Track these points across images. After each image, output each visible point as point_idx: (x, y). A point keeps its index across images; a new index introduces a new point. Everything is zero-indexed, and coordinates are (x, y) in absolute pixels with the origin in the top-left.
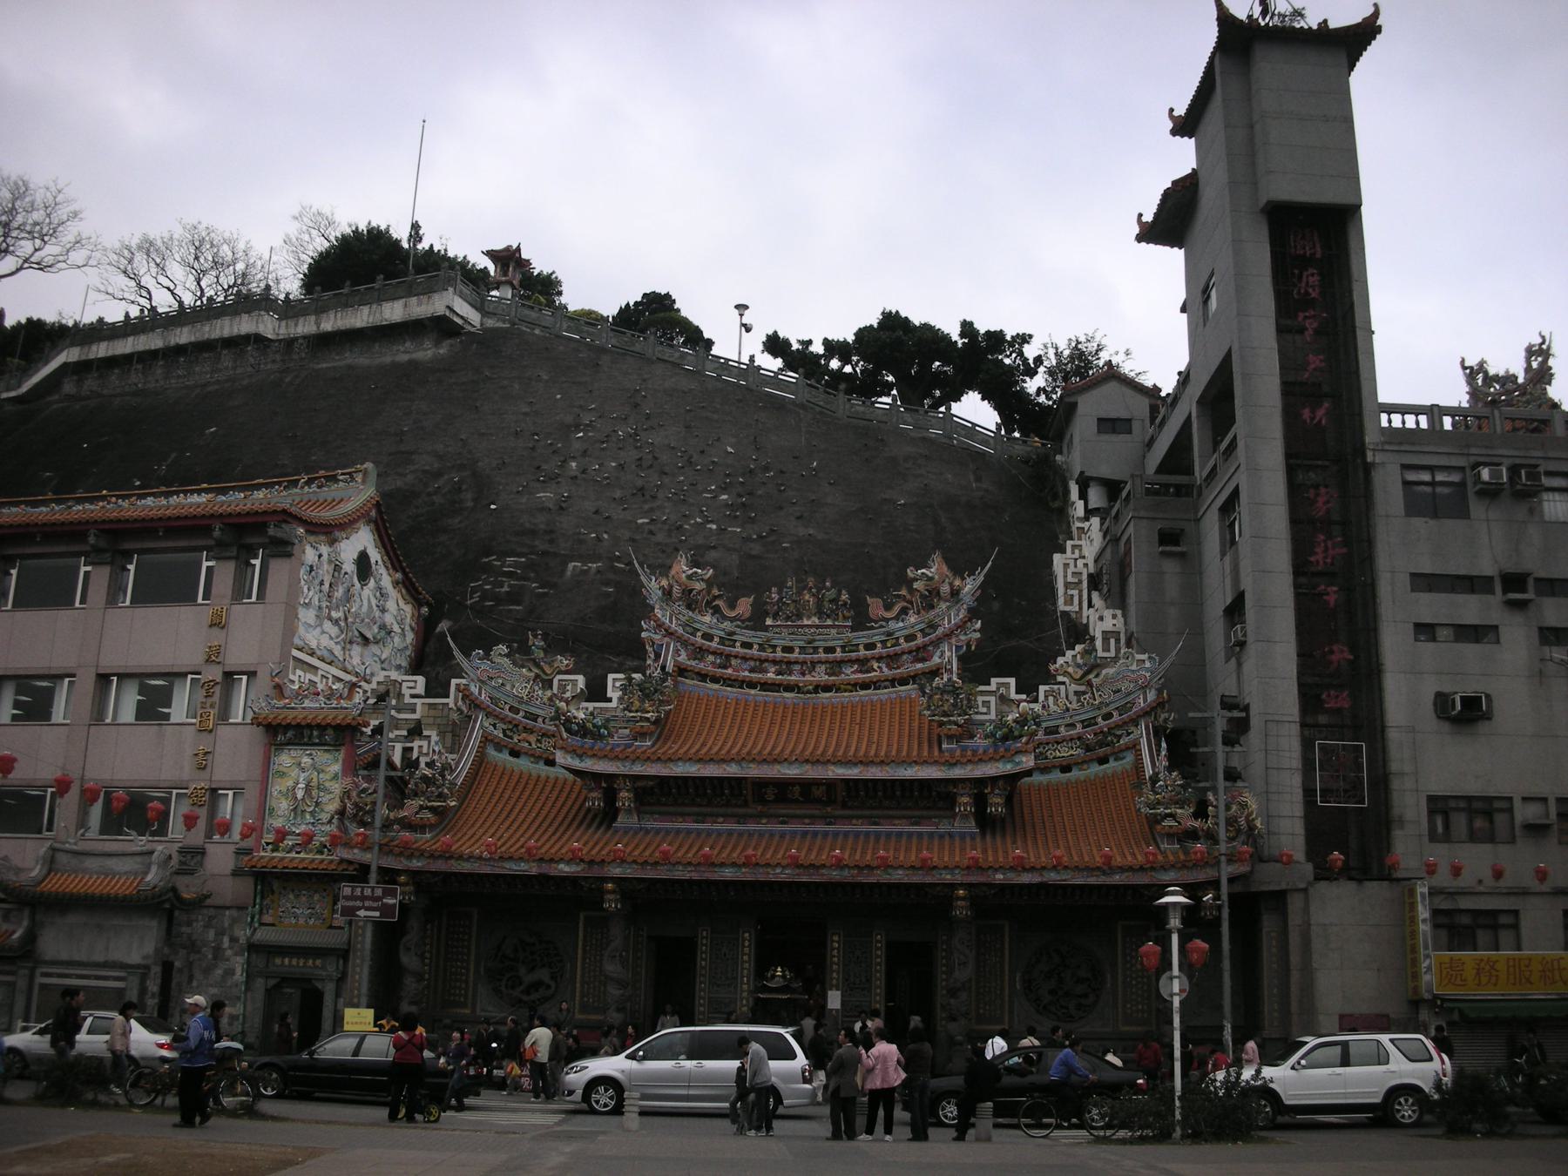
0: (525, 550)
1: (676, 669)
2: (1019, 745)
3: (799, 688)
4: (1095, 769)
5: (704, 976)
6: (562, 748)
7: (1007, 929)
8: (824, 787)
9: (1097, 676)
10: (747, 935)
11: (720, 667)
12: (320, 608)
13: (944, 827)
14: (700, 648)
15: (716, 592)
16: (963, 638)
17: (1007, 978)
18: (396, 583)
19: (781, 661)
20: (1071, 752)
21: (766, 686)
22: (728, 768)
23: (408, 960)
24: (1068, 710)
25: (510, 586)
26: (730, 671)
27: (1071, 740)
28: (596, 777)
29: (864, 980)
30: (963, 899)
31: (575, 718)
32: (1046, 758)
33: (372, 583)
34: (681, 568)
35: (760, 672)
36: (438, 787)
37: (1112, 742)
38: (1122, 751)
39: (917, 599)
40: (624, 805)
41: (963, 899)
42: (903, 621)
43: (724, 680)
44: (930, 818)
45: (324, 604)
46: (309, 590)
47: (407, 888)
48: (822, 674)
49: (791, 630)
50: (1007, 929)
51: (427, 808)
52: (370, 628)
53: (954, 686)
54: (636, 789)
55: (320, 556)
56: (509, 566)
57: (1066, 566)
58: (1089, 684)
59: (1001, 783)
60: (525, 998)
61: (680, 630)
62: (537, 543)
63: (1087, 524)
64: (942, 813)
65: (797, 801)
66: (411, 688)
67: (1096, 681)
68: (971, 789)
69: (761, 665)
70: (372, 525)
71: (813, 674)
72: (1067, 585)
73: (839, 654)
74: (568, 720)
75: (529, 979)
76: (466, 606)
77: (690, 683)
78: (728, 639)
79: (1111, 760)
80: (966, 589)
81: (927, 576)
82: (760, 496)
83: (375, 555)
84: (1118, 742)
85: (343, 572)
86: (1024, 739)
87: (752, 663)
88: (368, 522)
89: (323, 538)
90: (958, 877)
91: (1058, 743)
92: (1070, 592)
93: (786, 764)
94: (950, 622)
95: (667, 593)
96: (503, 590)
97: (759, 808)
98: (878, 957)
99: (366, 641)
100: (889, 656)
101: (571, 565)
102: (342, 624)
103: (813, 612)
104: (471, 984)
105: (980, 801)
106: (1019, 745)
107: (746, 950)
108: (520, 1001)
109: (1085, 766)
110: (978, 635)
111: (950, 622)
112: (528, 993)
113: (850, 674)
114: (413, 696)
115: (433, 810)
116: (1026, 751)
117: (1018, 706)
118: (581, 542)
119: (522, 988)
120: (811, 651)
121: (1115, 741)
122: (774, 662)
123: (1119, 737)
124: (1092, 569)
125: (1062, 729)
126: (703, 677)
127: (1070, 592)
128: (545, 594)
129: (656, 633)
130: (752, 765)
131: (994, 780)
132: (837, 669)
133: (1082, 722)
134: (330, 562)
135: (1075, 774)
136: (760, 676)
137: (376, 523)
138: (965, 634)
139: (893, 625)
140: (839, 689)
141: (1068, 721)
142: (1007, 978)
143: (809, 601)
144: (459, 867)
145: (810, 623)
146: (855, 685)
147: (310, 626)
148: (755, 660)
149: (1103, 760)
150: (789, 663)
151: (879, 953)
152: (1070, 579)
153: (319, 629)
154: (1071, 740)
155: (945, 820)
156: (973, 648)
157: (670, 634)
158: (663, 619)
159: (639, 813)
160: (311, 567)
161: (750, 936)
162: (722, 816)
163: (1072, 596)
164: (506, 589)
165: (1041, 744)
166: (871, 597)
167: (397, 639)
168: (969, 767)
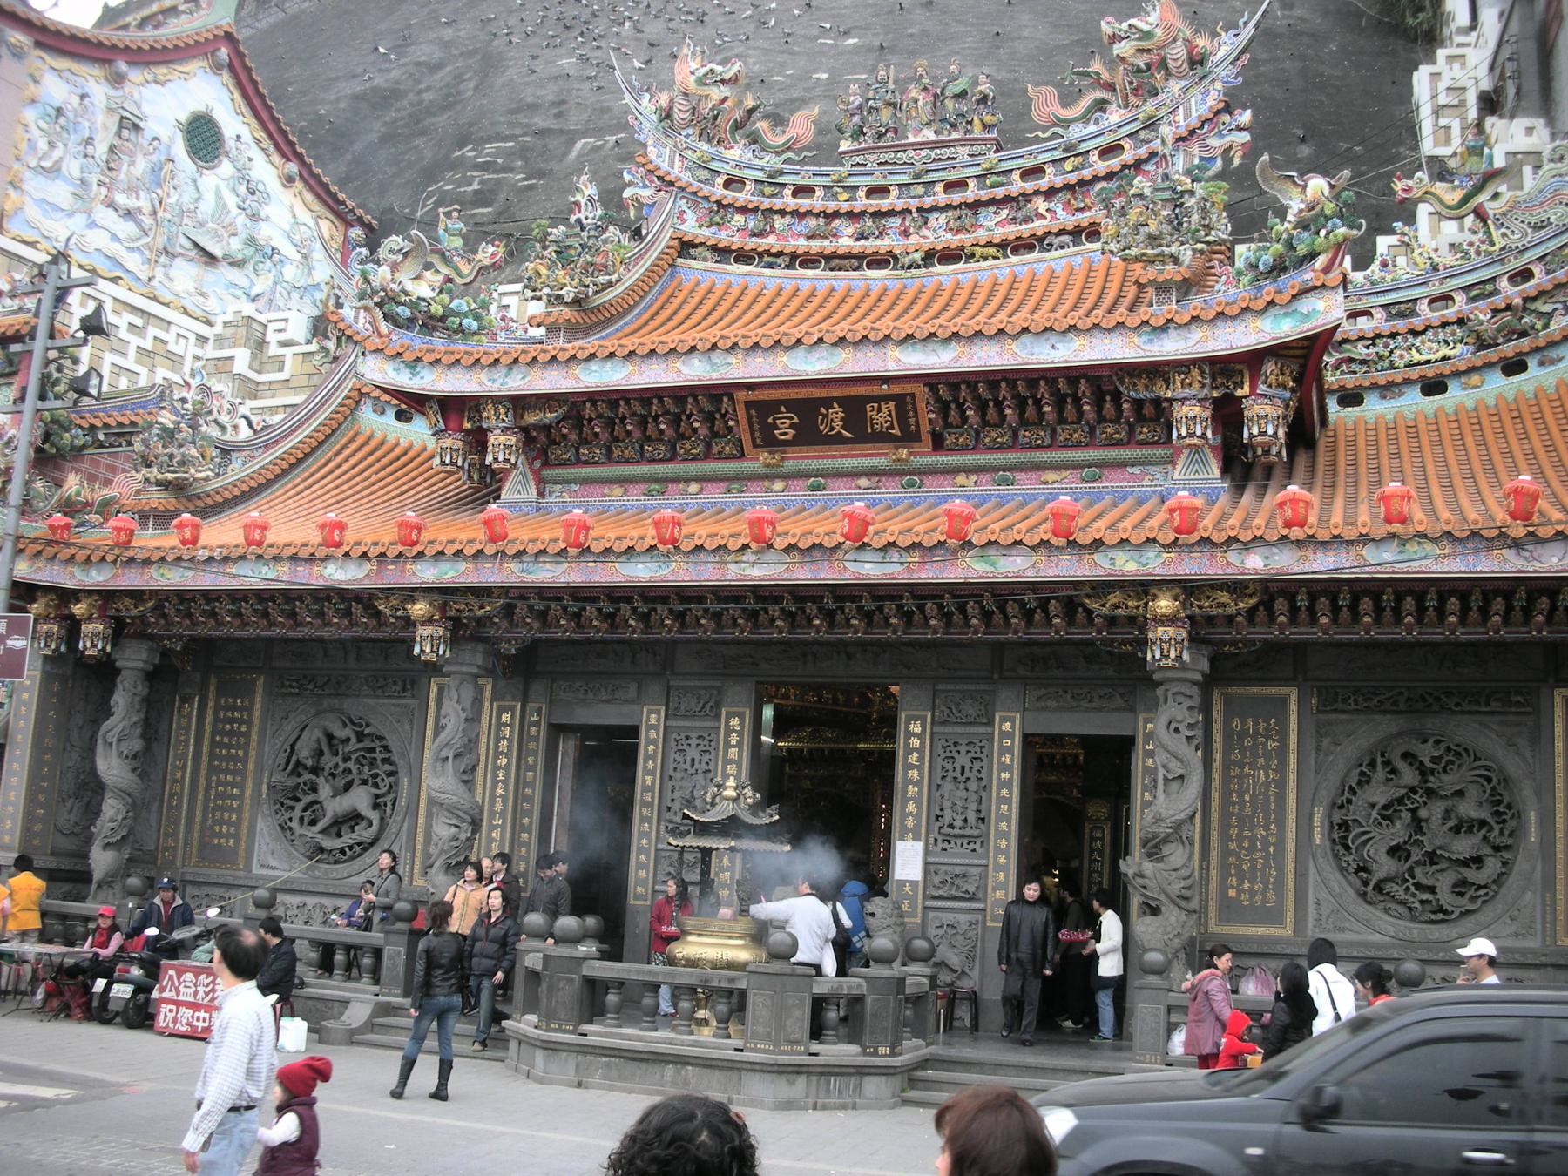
0: (517, 131)
1: (675, 243)
2: (1309, 275)
3: (895, 258)
4: (1496, 384)
5: (649, 805)
6: (378, 351)
7: (1293, 708)
8: (892, 404)
9: (1496, 196)
10: (735, 721)
11: (754, 235)
12: (83, 182)
13: (1153, 480)
14: (719, 203)
15: (750, 102)
16: (1214, 142)
17: (1292, 817)
18: (289, 180)
19: (863, 213)
20: (1445, 351)
21: (834, 260)
22: (685, 370)
23: (111, 767)
24: (1435, 268)
25: (482, 182)
26: (771, 239)
27: (1444, 325)
28: (451, 408)
29: (972, 816)
30: (1171, 620)
31: (407, 294)
32: (1392, 367)
33: (226, 168)
34: (689, 68)
35: (825, 237)
36: (181, 446)
37: (1532, 328)
38: (1553, 344)
39: (1121, 77)
40: (496, 460)
41: (1171, 620)
42: (1097, 122)
43: (761, 255)
44: (1122, 465)
45: (93, 179)
46: (51, 145)
47: (91, 626)
48: (941, 232)
49: (884, 157)
50: (1293, 708)
51: (158, 483)
52: (215, 235)
53: (1174, 191)
54: (525, 430)
55: (83, 97)
56: (488, 155)
57: (1436, 76)
58: (1480, 214)
59: (1270, 367)
60: (328, 843)
61: (686, 177)
62: (536, 120)
63: (1474, 34)
64: (1147, 452)
65: (838, 440)
66: (280, 331)
67: (1492, 208)
68: (1203, 386)
69: (827, 224)
70: (226, 75)
71: (924, 232)
72: (1438, 111)
73: (972, 193)
74: (392, 299)
75: (335, 806)
76: (413, 220)
77: (698, 269)
78: (773, 181)
79: (1532, 363)
80: (1221, 54)
81: (1140, 31)
82: (911, 35)
83: (234, 123)
84: (1546, 326)
85: (148, 135)
86: (1321, 261)
87: (811, 222)
88: (217, 68)
89: (96, 71)
90: (1155, 564)
91: (1415, 333)
92: (1442, 122)
93: (800, 351)
94: (1188, 115)
95: (667, 115)
96: (470, 189)
97: (764, 456)
98: (1004, 768)
99: (210, 258)
100: (1068, 187)
101: (579, 145)
102: (147, 221)
103: (925, 120)
104: (246, 815)
105: (1228, 415)
106: (1309, 275)
107: (733, 753)
108: (321, 850)
109: (1475, 379)
110: (1245, 137)
111: (1188, 115)
112: (339, 835)
113: (994, 225)
114: (284, 344)
115: (165, 485)
116: (1323, 286)
117: (1304, 188)
118: (604, 110)
119: (321, 825)
120: (920, 190)
121: (1539, 325)
122: (853, 216)
123: (1549, 316)
124: (1486, 85)
125: (1423, 307)
126: (723, 253)
127: (1442, 122)
128: (531, 187)
129: (645, 186)
130: (732, 359)
131: (1253, 360)
132: (968, 222)
133: (1466, 289)
134: (110, 110)
135: (1455, 394)
136: (826, 243)
137: (231, 68)
138: (1220, 135)
139: (1077, 131)
140: (973, 255)
141: (1436, 289)
142: (1292, 817)
143: (916, 101)
144: (163, 582)
145: (919, 139)
146: (1003, 245)
147: (57, 208)
148: (818, 215)
149: (1514, 366)
150: (878, 215)
151: (1007, 759)
152: (1443, 99)
153: (80, 220)
154: (1444, 325)
155: (1152, 469)
156: (1237, 162)
157: (666, 183)
158: (659, 162)
159: (541, 482)
160: (59, 111)
161: (742, 723)
162: (698, 479)
163: (1448, 128)
164: (476, 186)
165: (1379, 336)
166: (1036, 84)
167: (290, 273)
168: (1197, 334)
